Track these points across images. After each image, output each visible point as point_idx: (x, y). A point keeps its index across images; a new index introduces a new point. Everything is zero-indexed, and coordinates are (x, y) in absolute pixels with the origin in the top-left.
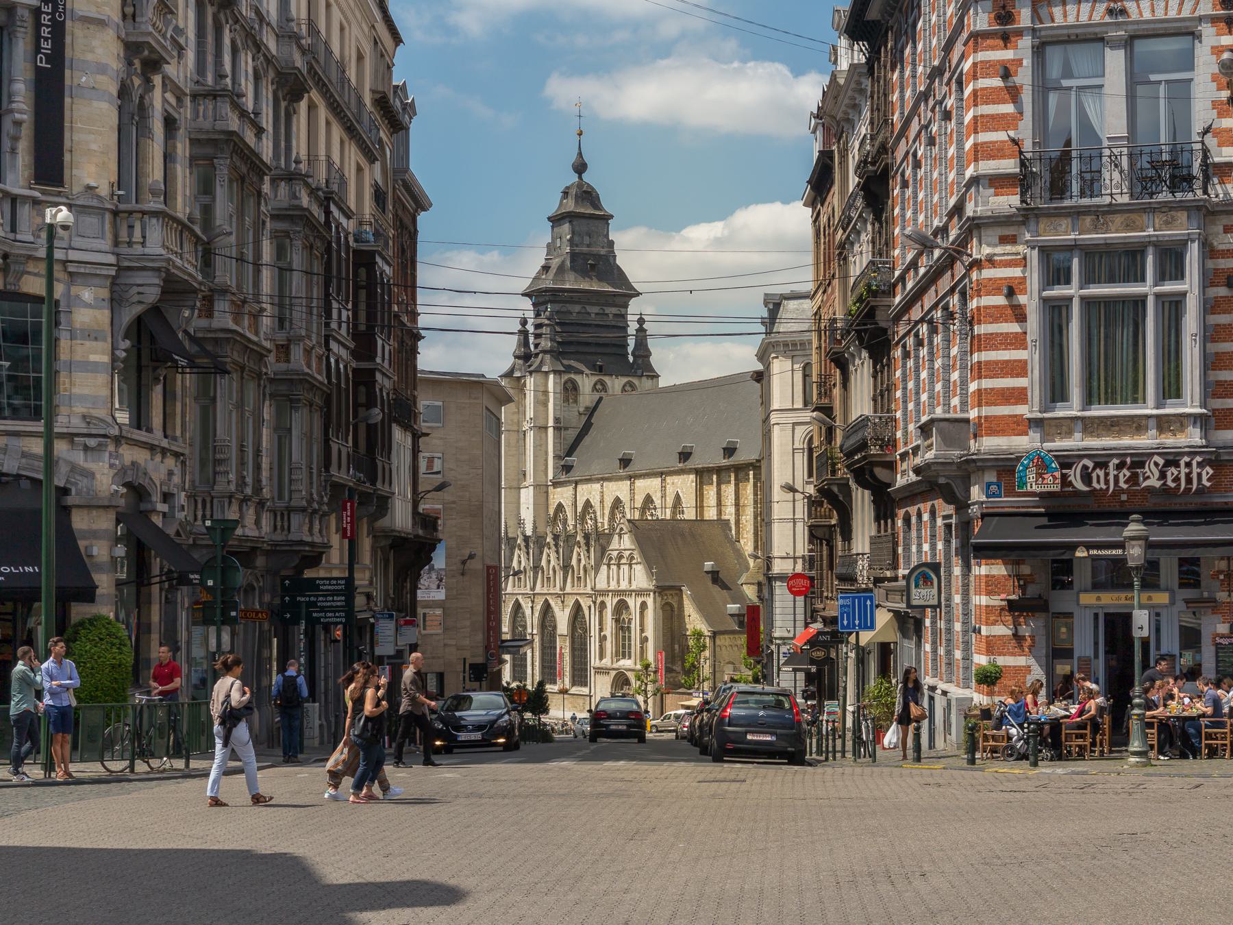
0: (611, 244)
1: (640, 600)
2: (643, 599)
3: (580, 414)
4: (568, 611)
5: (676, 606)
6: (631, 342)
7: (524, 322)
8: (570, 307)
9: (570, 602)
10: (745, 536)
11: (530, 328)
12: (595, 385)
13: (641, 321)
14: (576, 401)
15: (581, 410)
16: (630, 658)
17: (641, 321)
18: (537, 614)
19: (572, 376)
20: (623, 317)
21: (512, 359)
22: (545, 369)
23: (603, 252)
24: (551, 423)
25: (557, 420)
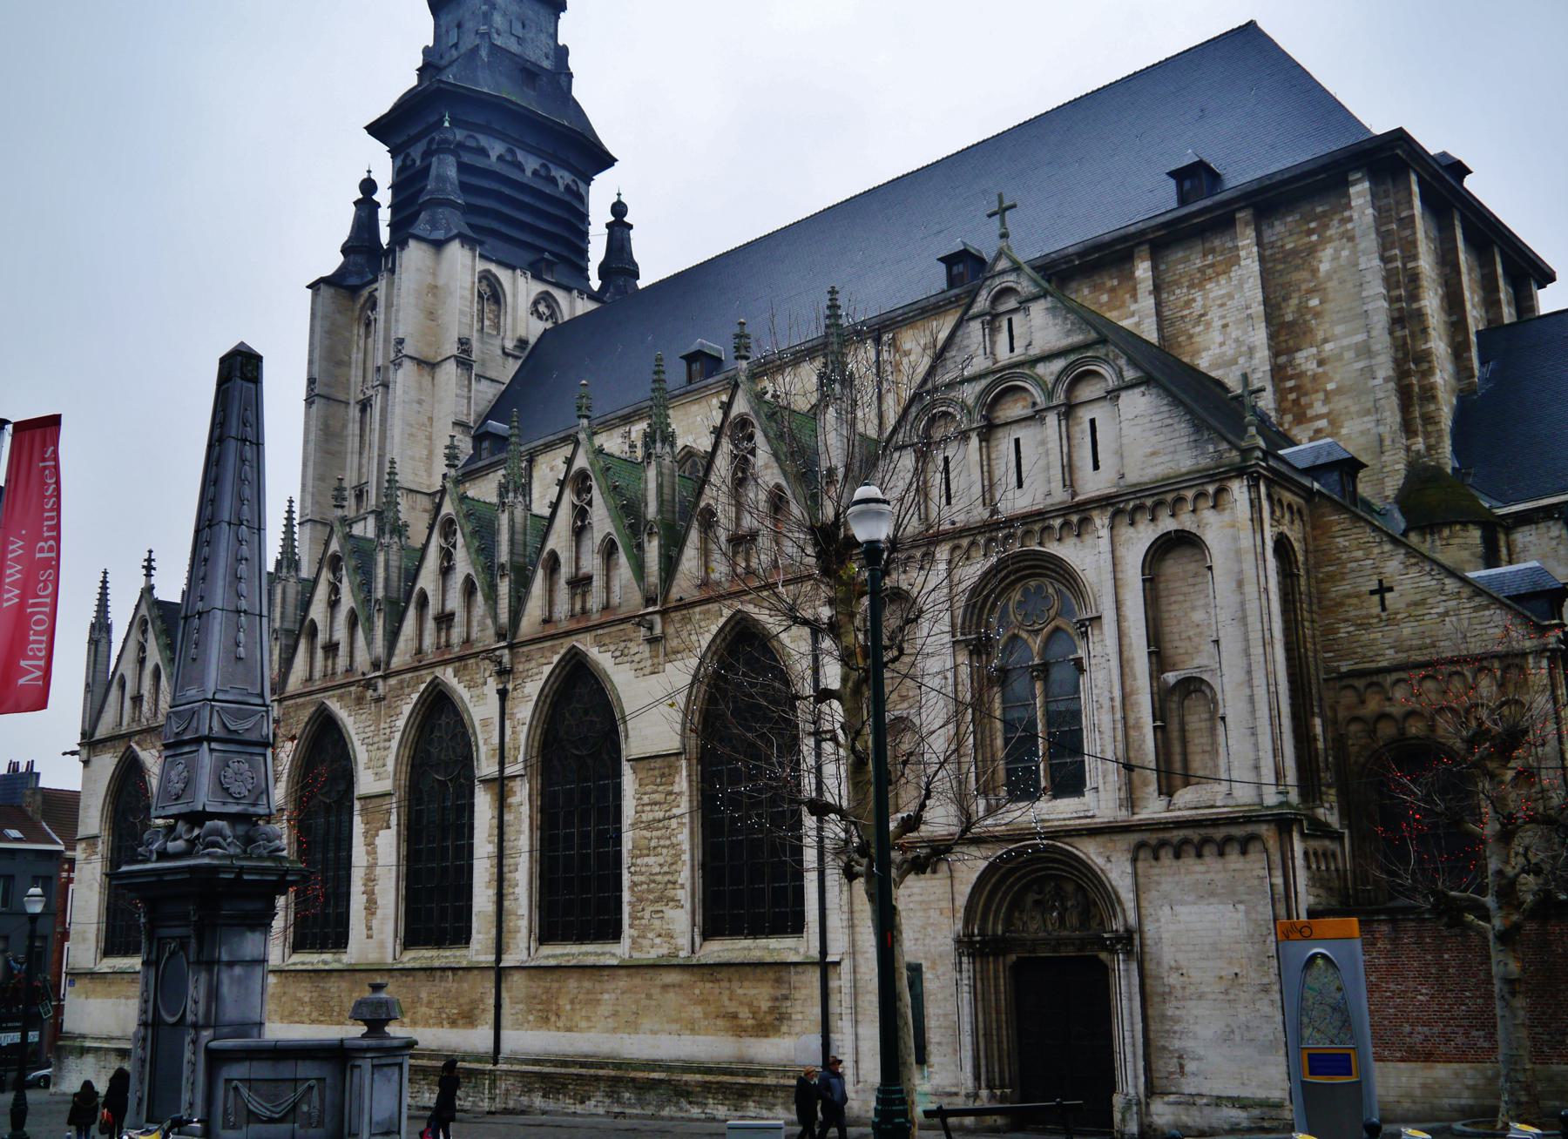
0: (563, 53)
1: (1140, 538)
2: (1167, 524)
3: (506, 354)
4: (679, 674)
5: (1301, 558)
6: (597, 250)
7: (368, 186)
8: (484, 141)
9: (707, 629)
10: (1319, 408)
11: (384, 196)
12: (536, 303)
13: (619, 209)
14: (497, 326)
15: (509, 345)
16: (1070, 782)
17: (619, 209)
18: (524, 711)
19: (493, 268)
20: (582, 199)
21: (340, 259)
22: (439, 235)
23: (546, 64)
24: (452, 348)
25: (464, 343)
